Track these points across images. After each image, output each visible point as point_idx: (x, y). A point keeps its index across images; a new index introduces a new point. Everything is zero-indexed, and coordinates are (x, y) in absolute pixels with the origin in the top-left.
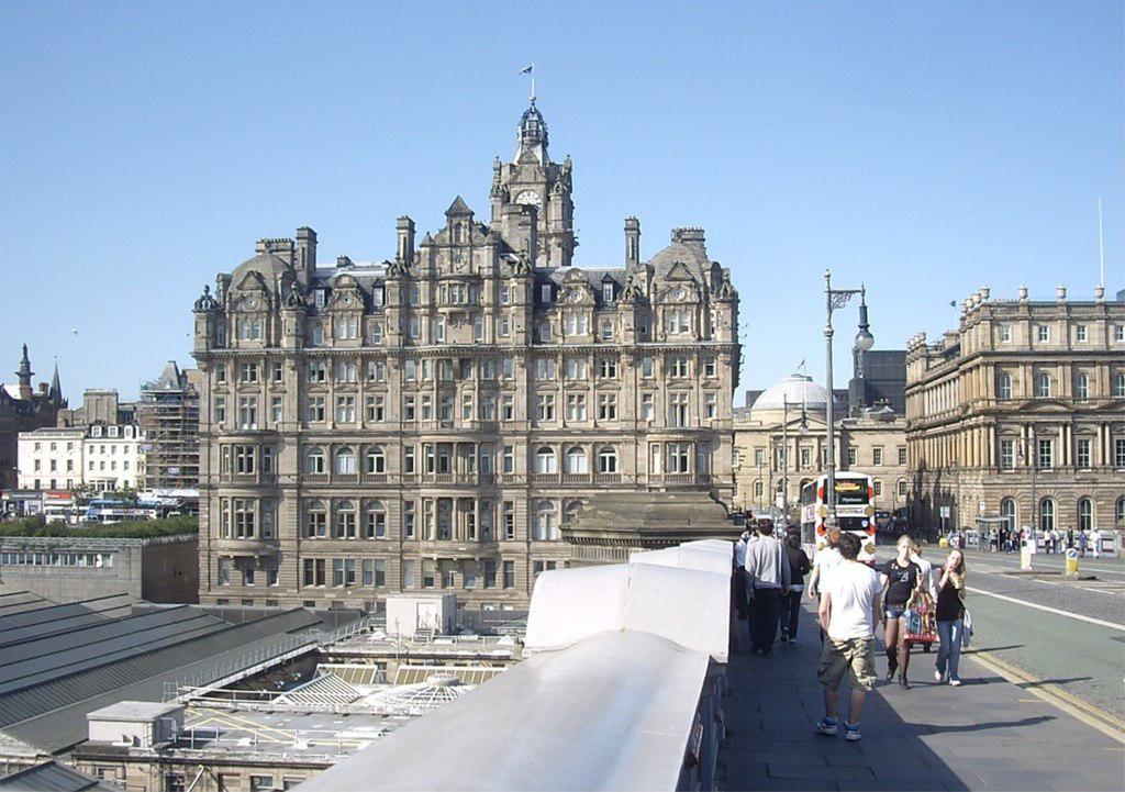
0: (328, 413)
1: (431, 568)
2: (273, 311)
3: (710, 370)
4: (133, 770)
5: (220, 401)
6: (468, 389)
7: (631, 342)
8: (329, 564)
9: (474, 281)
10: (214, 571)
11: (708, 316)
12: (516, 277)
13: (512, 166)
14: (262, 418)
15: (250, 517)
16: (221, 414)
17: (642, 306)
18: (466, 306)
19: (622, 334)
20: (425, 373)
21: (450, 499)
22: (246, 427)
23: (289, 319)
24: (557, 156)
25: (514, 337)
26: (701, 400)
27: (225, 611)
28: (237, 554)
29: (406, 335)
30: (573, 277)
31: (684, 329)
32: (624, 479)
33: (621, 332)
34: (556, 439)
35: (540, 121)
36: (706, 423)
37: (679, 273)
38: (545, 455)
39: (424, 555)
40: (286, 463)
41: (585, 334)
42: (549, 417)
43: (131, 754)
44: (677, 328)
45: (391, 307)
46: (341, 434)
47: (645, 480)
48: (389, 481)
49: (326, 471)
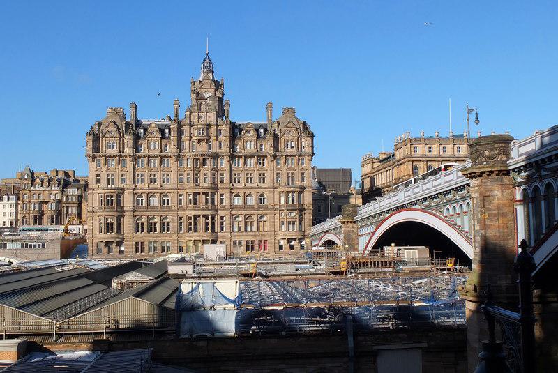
2: (121, 137)
3: (303, 163)
5: (98, 175)
6: (206, 170)
10: (95, 248)
13: (200, 82)
15: (112, 224)
16: (98, 181)
17: (276, 138)
20: (188, 164)
22: (109, 186)
23: (128, 140)
25: (225, 149)
28: (107, 240)
29: (180, 148)
30: (248, 126)
31: (292, 147)
33: (268, 147)
35: (210, 63)
36: (302, 184)
40: (127, 200)
41: (252, 148)
47: (278, 207)
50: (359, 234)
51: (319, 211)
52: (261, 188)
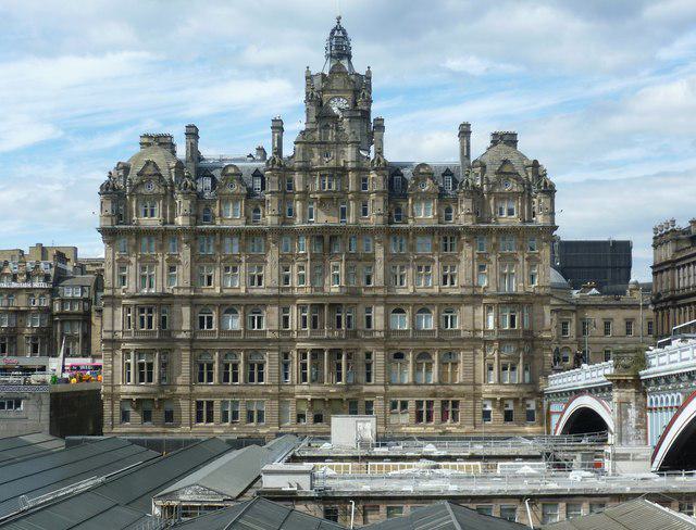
0: (216, 279)
1: (304, 408)
4: (300, 507)
7: (469, 223)
8: (217, 403)
9: (340, 172)
10: (117, 411)
11: (530, 202)
12: (375, 169)
14: (160, 283)
15: (150, 366)
18: (335, 192)
19: (462, 217)
21: (322, 351)
24: (359, 67)
25: (374, 219)
26: (526, 270)
27: (148, 441)
29: (286, 214)
30: (422, 170)
32: (463, 335)
34: (408, 300)
37: (507, 169)
38: (398, 315)
39: (299, 396)
42: (401, 284)
43: (299, 495)
44: (505, 211)
45: (271, 192)
46: (228, 297)
47: (481, 335)
48: (269, 336)
49: (215, 327)
50: (649, 405)
51: (565, 332)
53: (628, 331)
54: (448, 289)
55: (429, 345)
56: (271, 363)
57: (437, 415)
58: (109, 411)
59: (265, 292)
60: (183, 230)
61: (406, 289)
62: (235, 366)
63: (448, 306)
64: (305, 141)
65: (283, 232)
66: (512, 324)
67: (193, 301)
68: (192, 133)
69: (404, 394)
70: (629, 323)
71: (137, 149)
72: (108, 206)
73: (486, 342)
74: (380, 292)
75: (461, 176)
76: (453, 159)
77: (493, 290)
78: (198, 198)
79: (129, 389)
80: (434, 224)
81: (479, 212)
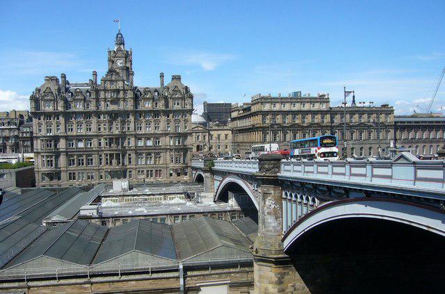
0: (74, 130)
4: (93, 221)
7: (164, 109)
8: (76, 172)
9: (118, 91)
15: (52, 161)
16: (40, 130)
24: (127, 48)
29: (98, 106)
37: (176, 89)
47: (168, 147)
48: (94, 149)
51: (204, 139)
52: (156, 134)
53: (226, 138)
54: (157, 132)
55: (150, 151)
56: (95, 158)
57: (154, 174)
58: (38, 177)
59: (92, 134)
60: (61, 112)
61: (143, 132)
62: (83, 160)
63: (156, 137)
64: (104, 81)
65: (98, 114)
66: (179, 143)
67: (67, 138)
68: (64, 76)
69: (143, 168)
70: (226, 135)
71: (44, 82)
72: (33, 104)
73: (170, 150)
74: (133, 133)
75: (161, 92)
76: (157, 85)
77: (172, 131)
78: (66, 101)
79: (46, 169)
80: (151, 109)
81: (167, 105)
